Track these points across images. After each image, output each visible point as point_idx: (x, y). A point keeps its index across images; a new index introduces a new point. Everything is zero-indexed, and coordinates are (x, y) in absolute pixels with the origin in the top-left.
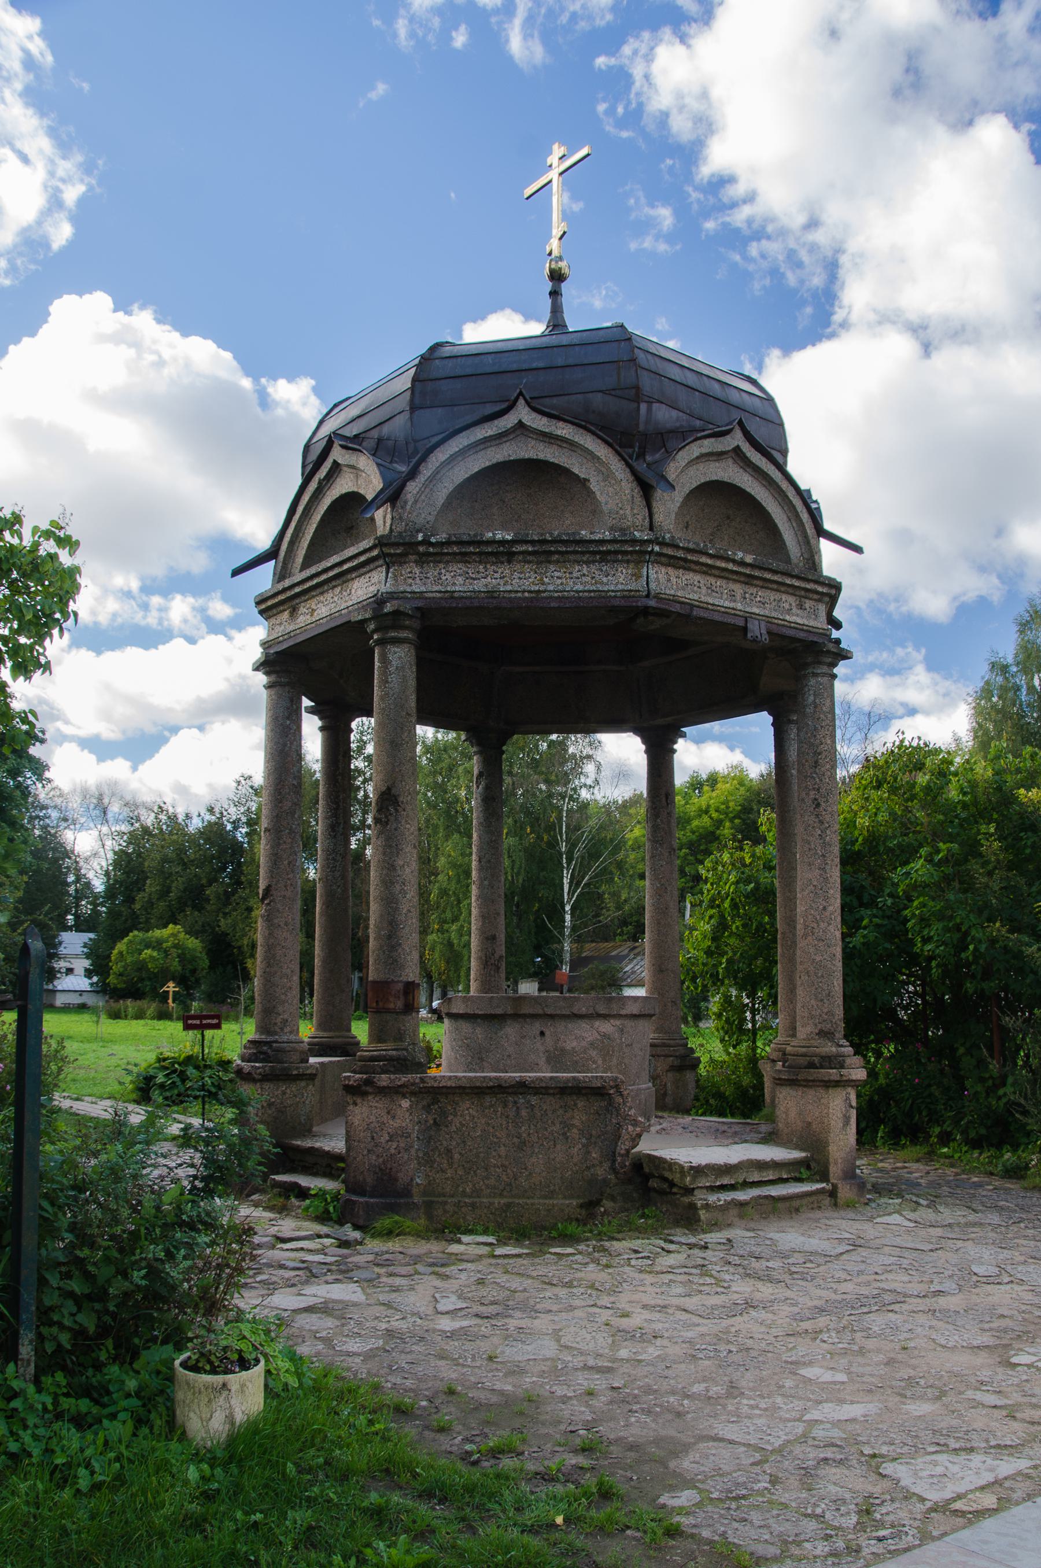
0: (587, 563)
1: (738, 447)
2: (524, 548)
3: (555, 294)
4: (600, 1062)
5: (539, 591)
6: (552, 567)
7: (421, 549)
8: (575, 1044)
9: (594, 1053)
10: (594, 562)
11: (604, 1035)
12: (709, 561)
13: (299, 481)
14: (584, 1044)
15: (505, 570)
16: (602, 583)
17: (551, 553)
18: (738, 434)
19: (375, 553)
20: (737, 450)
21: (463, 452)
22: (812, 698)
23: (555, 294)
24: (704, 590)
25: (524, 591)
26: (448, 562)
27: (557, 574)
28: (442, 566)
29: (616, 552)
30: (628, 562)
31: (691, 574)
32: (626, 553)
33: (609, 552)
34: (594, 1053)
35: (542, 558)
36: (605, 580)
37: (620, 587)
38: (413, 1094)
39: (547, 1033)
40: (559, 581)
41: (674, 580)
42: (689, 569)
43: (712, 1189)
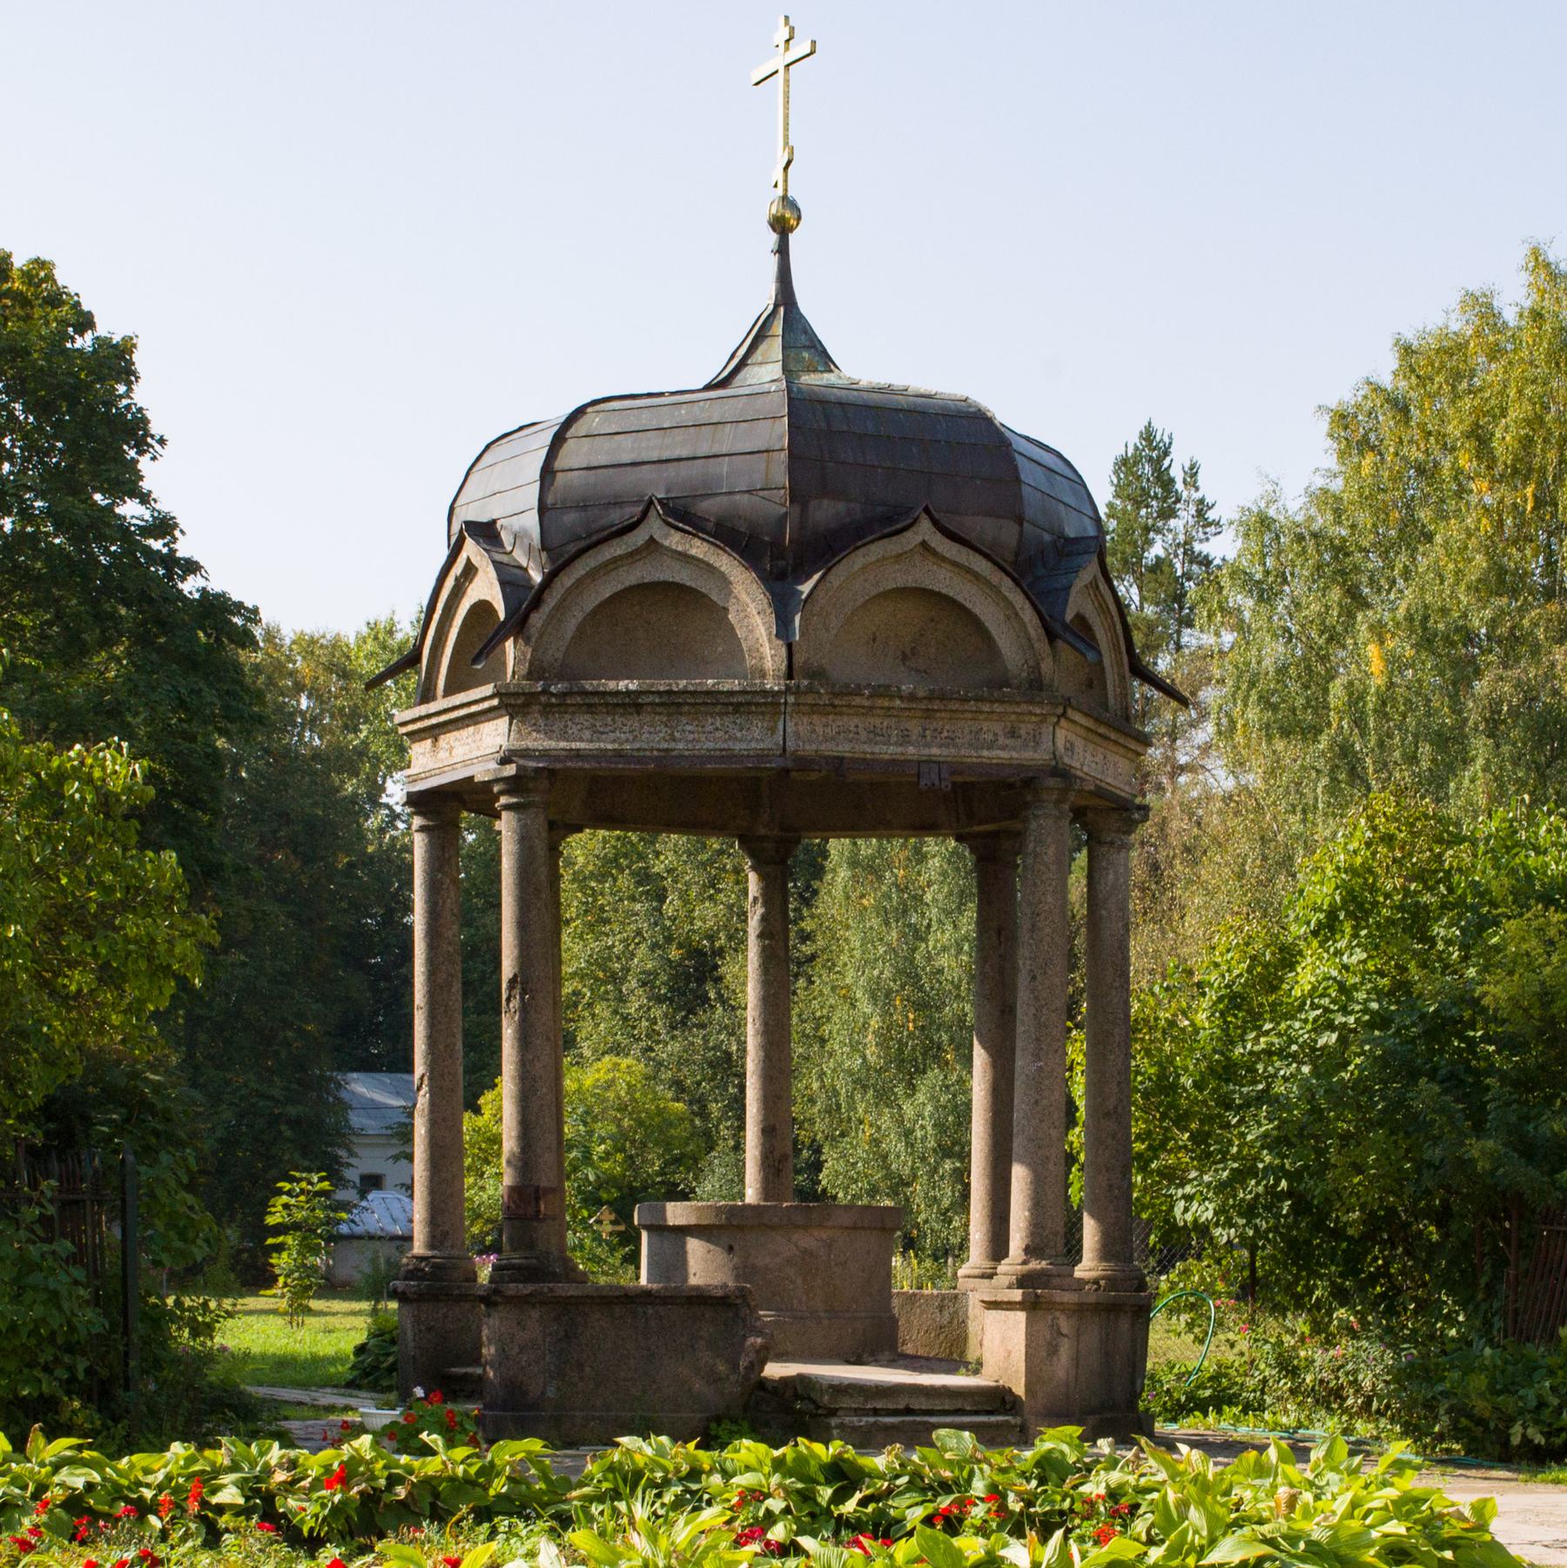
0: (721, 714)
1: (924, 544)
2: (650, 699)
3: (783, 251)
4: (799, 1281)
5: (667, 750)
6: (684, 720)
7: (543, 699)
8: (768, 1260)
9: (791, 1272)
10: (727, 714)
11: (805, 1251)
12: (866, 703)
13: (444, 553)
14: (778, 1260)
15: (634, 722)
16: (736, 739)
17: (679, 705)
18: (925, 525)
19: (495, 702)
20: (924, 544)
21: (593, 575)
22: (1031, 846)
23: (783, 251)
24: (863, 736)
25: (652, 750)
26: (573, 713)
27: (689, 728)
28: (568, 717)
29: (749, 704)
30: (763, 713)
31: (846, 719)
32: (757, 704)
33: (740, 704)
34: (791, 1272)
35: (673, 709)
36: (739, 735)
37: (753, 745)
38: (542, 1303)
39: (736, 1247)
40: (691, 737)
41: (820, 730)
42: (841, 714)
43: (858, 1412)
